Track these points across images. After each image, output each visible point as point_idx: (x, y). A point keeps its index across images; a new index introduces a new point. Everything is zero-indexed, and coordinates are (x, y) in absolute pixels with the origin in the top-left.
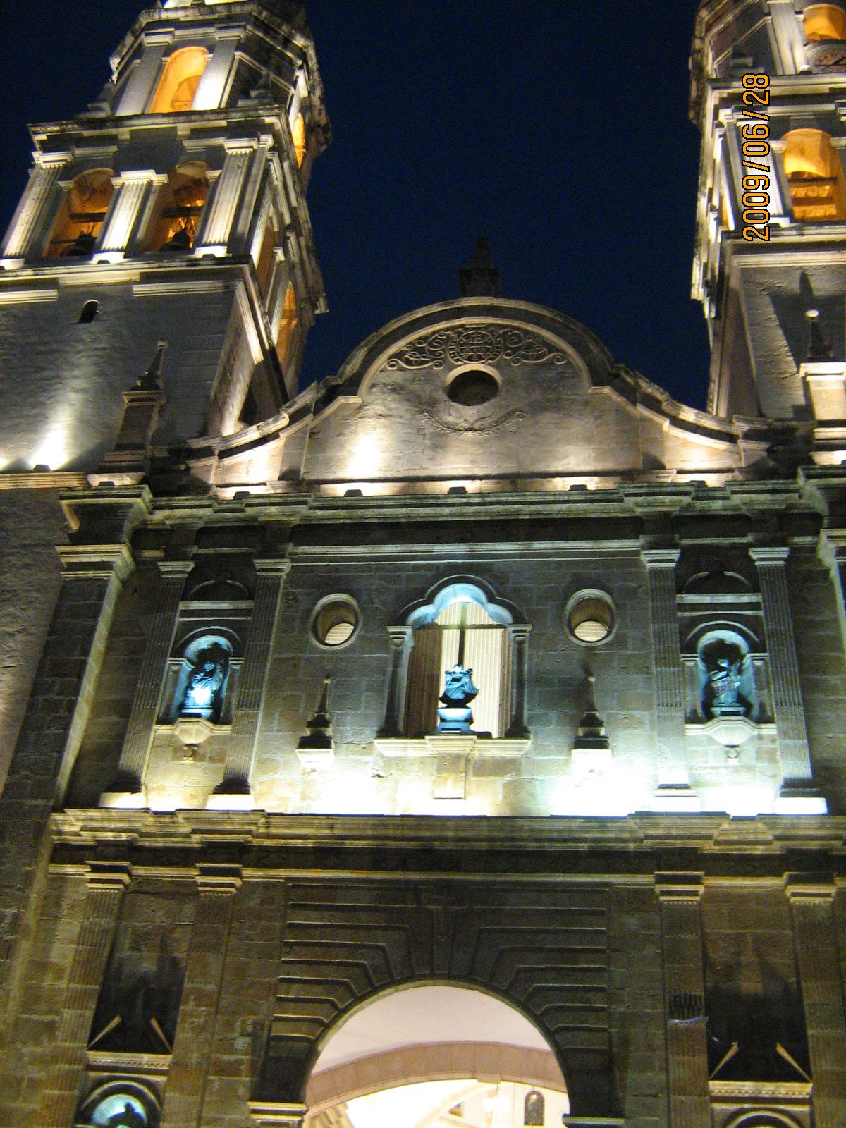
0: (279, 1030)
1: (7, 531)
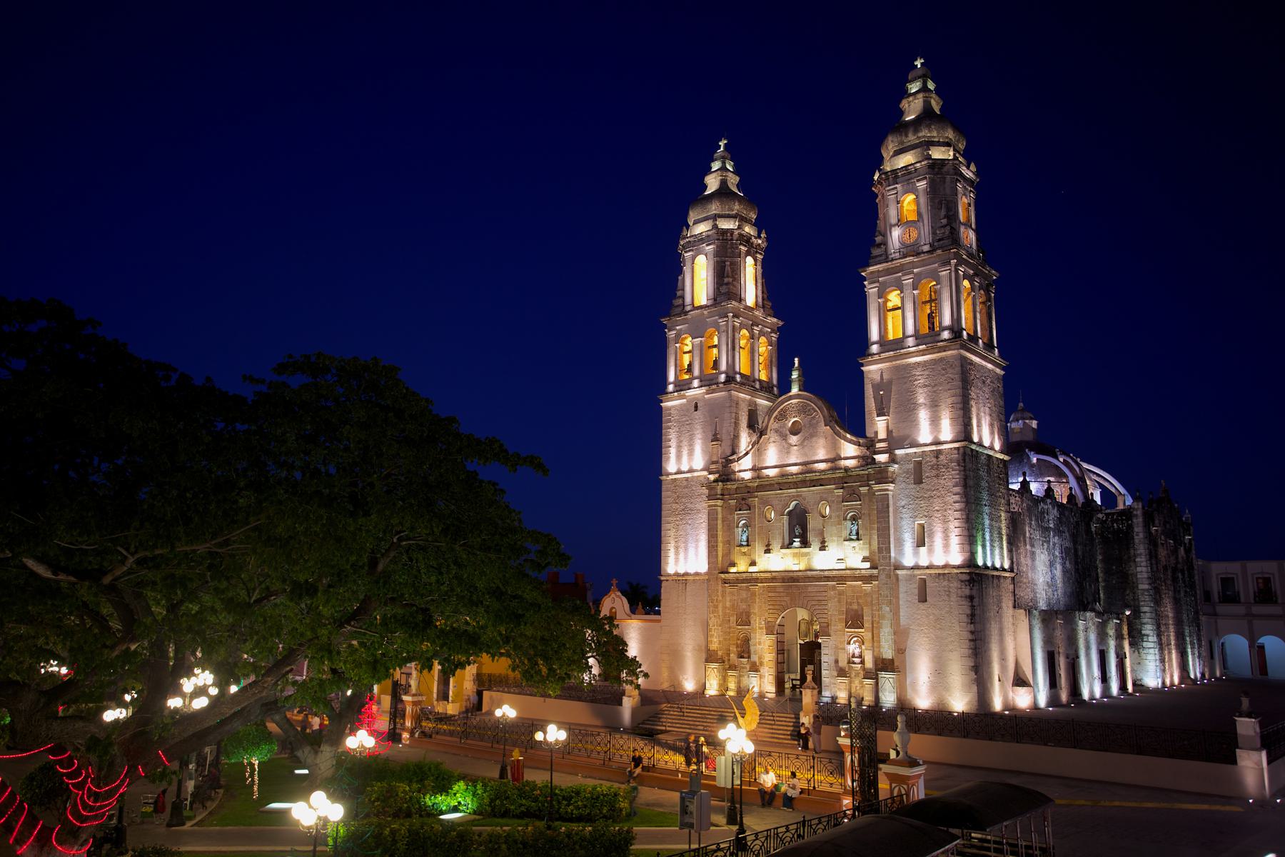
0: (769, 620)
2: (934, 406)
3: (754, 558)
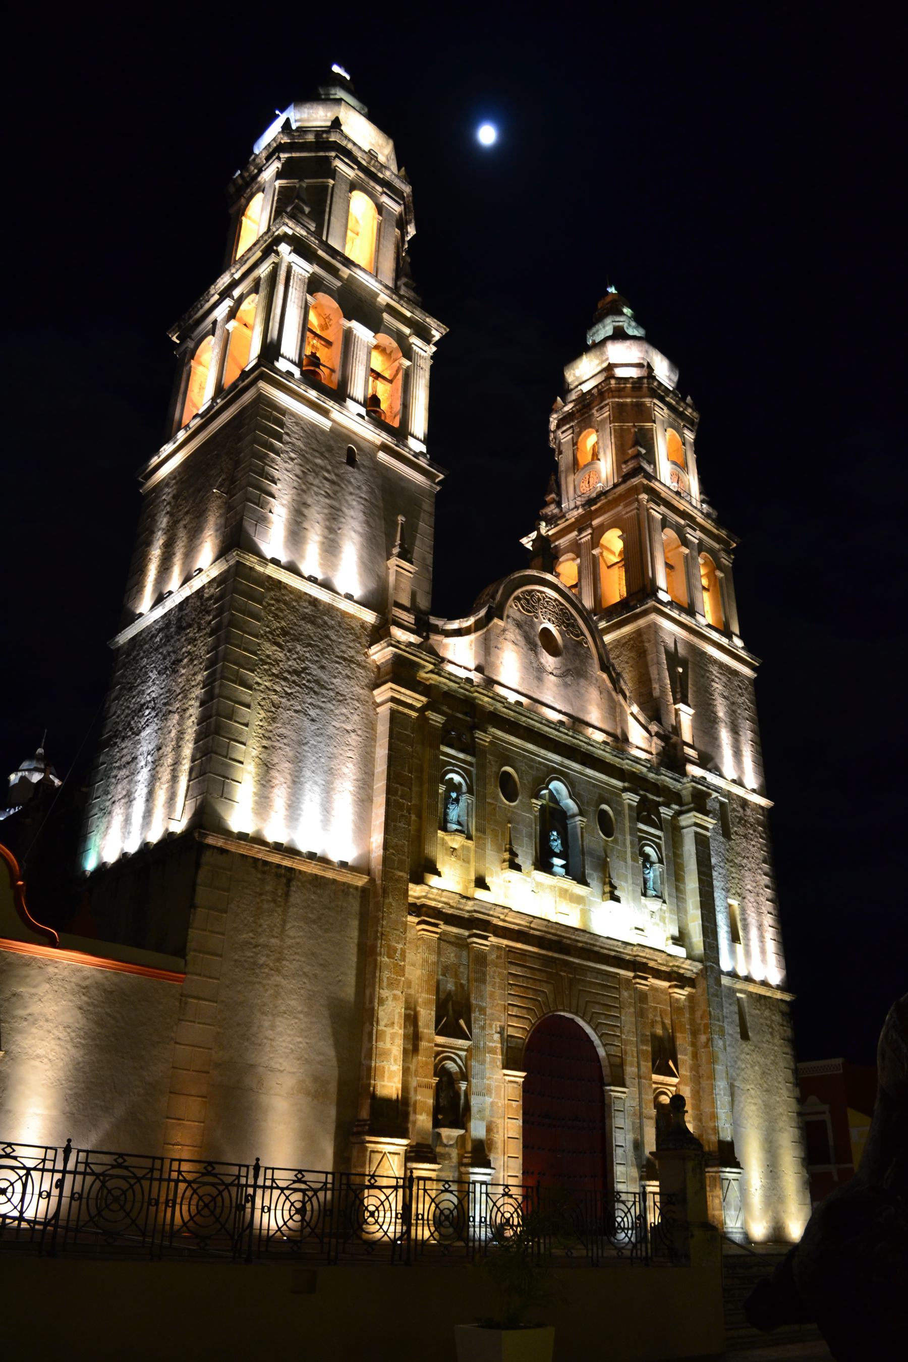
0: (511, 1032)
1: (331, 640)
2: (735, 731)
3: (482, 873)
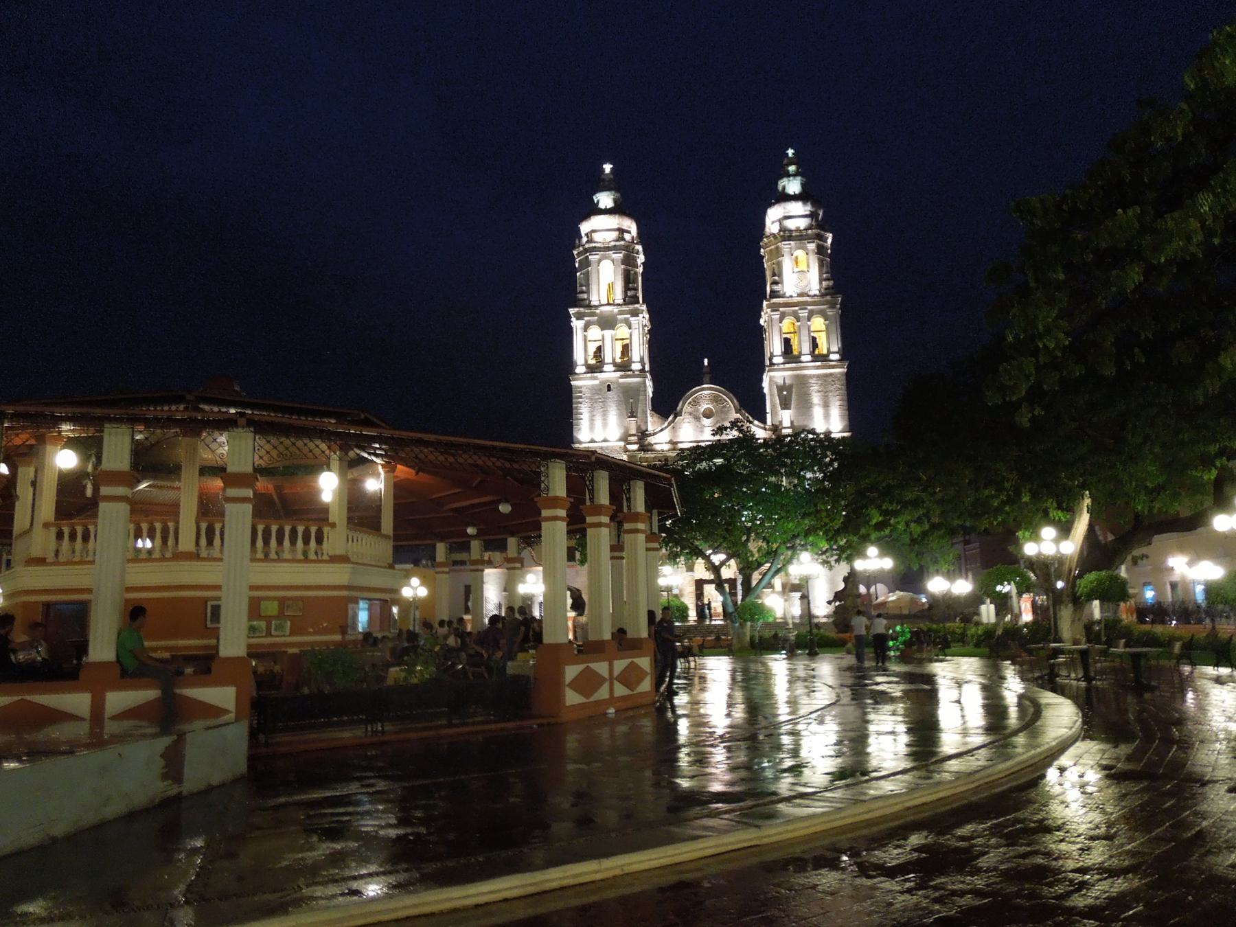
2: (826, 405)
